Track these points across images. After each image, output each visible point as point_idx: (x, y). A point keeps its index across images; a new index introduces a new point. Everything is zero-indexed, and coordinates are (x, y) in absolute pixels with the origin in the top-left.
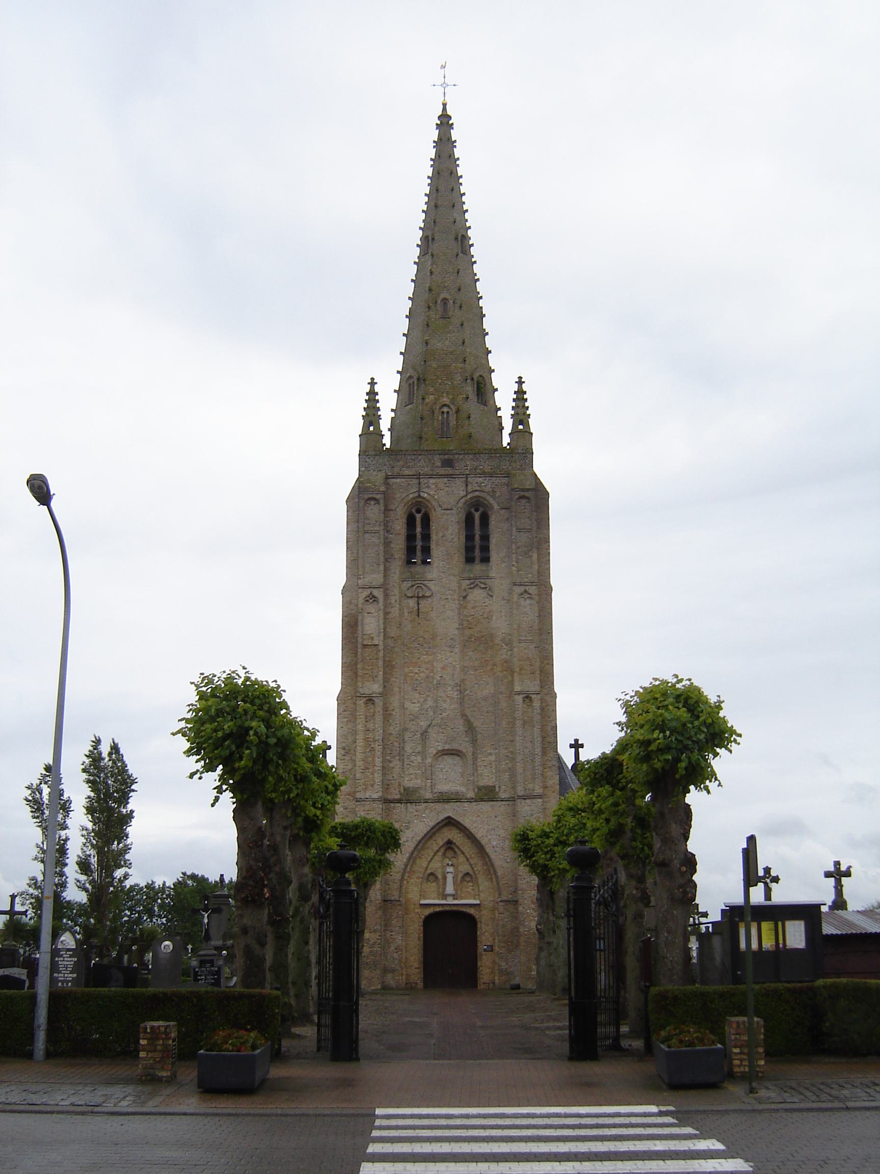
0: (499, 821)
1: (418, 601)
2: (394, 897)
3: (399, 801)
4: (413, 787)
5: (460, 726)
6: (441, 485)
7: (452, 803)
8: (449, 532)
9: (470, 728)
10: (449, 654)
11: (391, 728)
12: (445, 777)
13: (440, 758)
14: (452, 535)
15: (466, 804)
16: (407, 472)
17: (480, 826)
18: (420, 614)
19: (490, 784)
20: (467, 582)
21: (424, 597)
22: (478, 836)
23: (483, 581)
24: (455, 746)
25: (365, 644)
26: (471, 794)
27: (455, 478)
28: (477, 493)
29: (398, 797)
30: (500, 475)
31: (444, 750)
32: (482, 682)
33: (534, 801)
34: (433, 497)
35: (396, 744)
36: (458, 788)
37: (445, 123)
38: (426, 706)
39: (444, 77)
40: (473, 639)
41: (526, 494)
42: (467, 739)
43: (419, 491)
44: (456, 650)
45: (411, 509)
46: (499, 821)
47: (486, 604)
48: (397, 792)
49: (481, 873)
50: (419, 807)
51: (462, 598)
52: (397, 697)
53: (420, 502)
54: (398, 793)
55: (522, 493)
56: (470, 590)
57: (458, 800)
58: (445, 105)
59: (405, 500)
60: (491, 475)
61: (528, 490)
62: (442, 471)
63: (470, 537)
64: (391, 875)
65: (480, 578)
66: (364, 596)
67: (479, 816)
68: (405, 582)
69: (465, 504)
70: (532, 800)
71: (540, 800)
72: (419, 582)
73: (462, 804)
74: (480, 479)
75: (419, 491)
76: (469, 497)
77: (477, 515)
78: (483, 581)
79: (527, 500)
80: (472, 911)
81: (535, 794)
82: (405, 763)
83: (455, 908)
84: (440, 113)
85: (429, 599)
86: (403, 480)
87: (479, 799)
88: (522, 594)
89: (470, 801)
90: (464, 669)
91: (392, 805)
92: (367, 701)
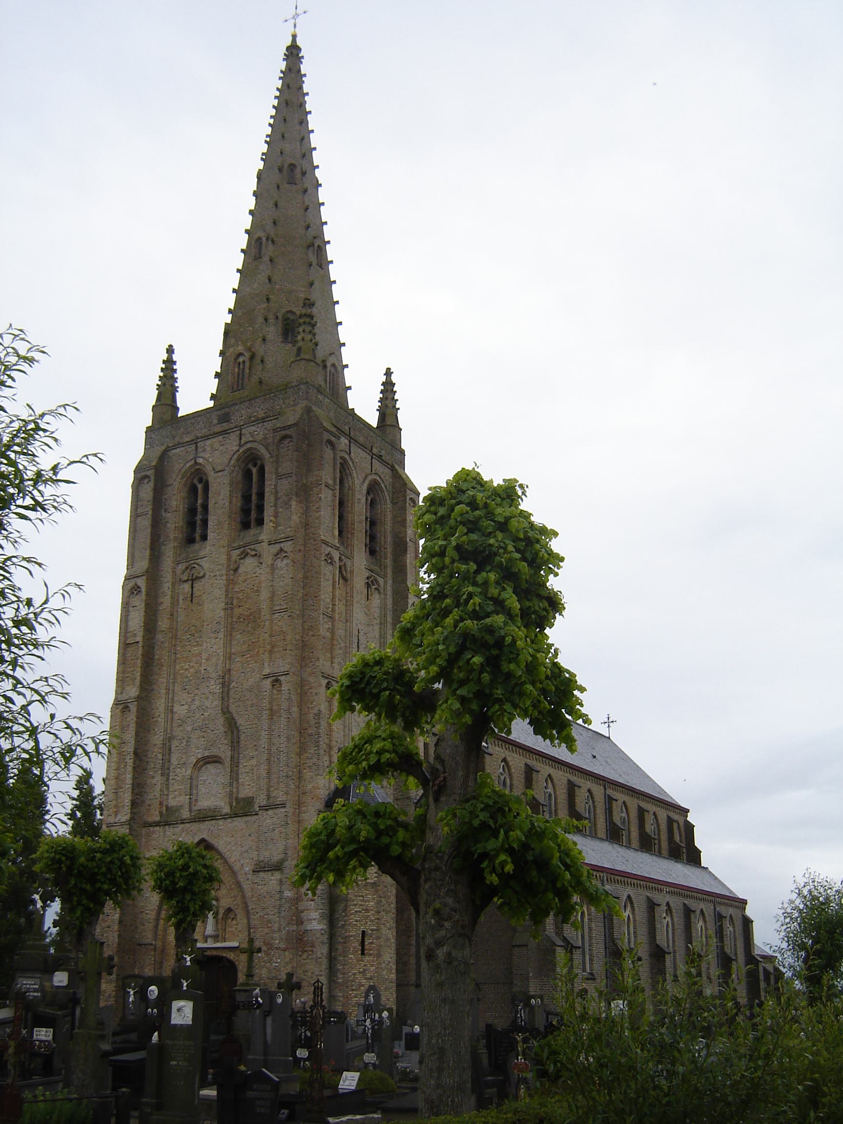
0: (252, 840)
1: (192, 584)
2: (147, 940)
3: (157, 824)
4: (176, 806)
5: (220, 725)
6: (216, 446)
7: (207, 822)
8: (221, 497)
9: (232, 725)
10: (214, 641)
11: (157, 737)
12: (207, 791)
13: (203, 768)
14: (223, 499)
15: (221, 822)
16: (187, 439)
17: (234, 848)
18: (194, 599)
19: (250, 795)
20: (238, 552)
21: (198, 578)
22: (231, 860)
23: (252, 547)
24: (214, 751)
25: (128, 642)
26: (226, 810)
27: (229, 433)
28: (249, 445)
29: (157, 819)
30: (272, 418)
31: (204, 758)
32: (248, 670)
33: (276, 811)
34: (208, 461)
35: (160, 756)
36: (218, 803)
37: (293, 53)
38: (193, 707)
39: (296, 8)
40: (242, 620)
41: (288, 432)
42: (225, 742)
43: (195, 458)
44: (221, 635)
45: (193, 480)
46: (252, 840)
47: (257, 575)
48: (157, 813)
49: (240, 907)
50: (176, 829)
51: (232, 572)
52: (163, 700)
53: (199, 469)
54: (158, 814)
55: (283, 433)
56: (242, 561)
57: (213, 818)
58: (294, 37)
59: (183, 470)
60: (263, 420)
61: (289, 427)
62: (218, 429)
63: (247, 498)
64: (147, 914)
65: (250, 544)
66: (129, 588)
67: (233, 836)
68: (180, 565)
69: (238, 460)
70: (274, 810)
71: (283, 810)
72: (192, 562)
73: (217, 821)
74: (253, 428)
75: (195, 458)
76: (241, 451)
77: (254, 471)
78: (252, 547)
79: (288, 440)
80: (231, 956)
81: (278, 803)
82: (171, 778)
83: (215, 953)
84: (289, 44)
85: (203, 580)
86: (182, 448)
87: (234, 815)
88: (278, 554)
89: (225, 817)
90: (229, 657)
91: (152, 829)
92: (124, 708)
